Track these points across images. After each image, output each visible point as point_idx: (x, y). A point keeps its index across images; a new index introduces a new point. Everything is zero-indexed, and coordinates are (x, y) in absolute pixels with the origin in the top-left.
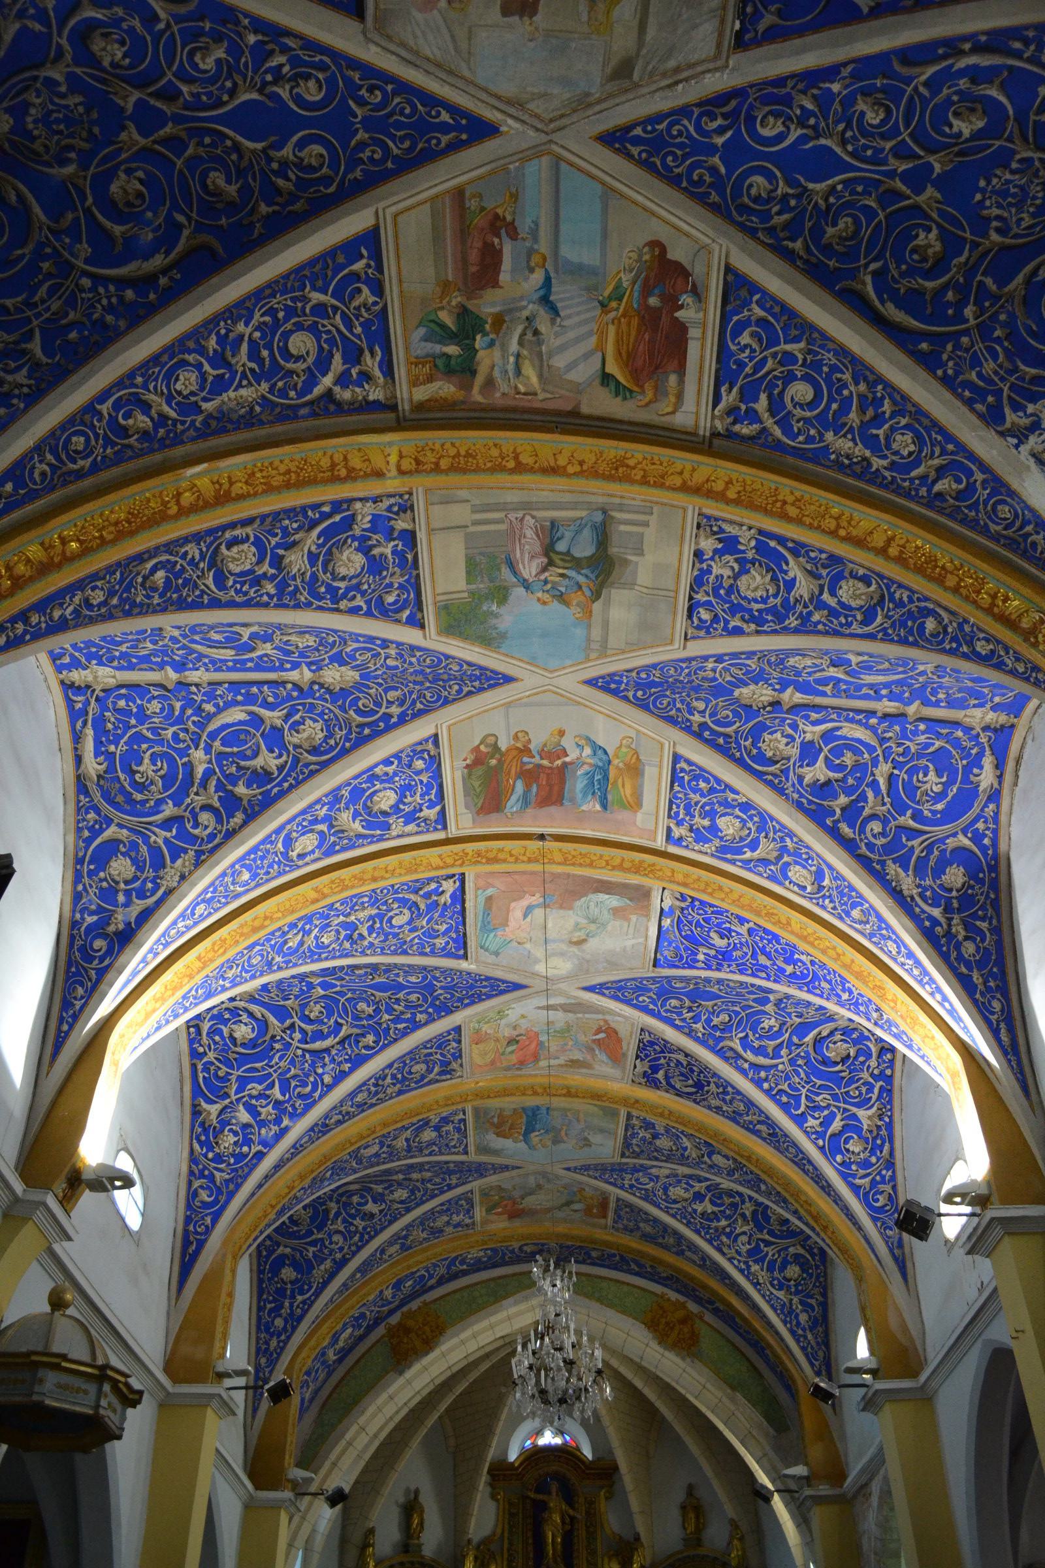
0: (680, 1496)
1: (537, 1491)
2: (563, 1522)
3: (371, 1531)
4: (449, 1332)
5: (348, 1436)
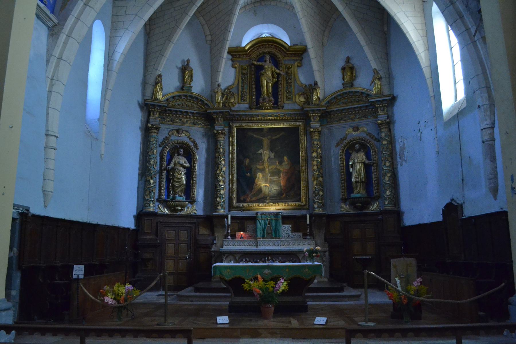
0: (341, 63)
1: (258, 61)
2: (273, 77)
3: (160, 76)
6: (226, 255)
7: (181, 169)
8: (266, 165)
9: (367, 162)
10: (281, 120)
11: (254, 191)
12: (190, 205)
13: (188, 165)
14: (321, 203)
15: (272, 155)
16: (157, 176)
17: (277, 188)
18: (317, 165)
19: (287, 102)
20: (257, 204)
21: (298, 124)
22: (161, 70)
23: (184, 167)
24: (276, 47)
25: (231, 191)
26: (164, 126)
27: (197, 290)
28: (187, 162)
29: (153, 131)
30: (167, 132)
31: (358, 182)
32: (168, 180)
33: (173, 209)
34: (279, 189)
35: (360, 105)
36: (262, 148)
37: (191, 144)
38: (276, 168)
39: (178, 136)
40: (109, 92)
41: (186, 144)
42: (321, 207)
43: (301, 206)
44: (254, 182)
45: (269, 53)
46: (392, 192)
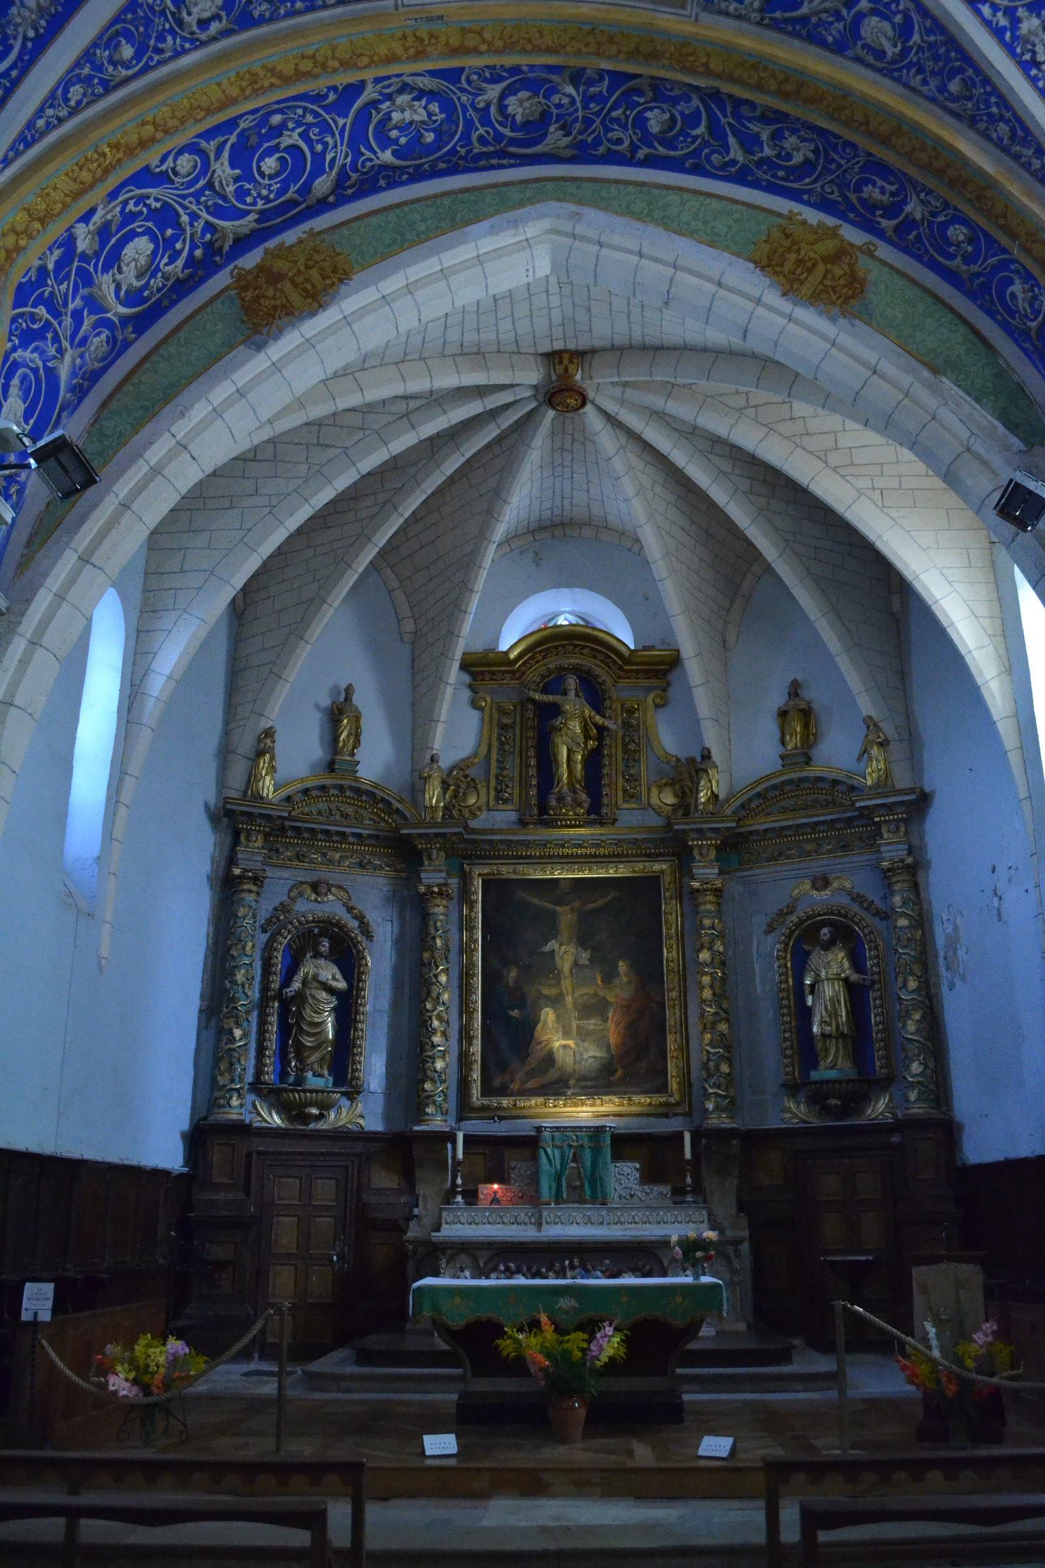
0: (777, 698)
1: (545, 691)
2: (587, 737)
3: (269, 733)
4: (357, 278)
5: (155, 454)
6: (449, 1252)
7: (323, 995)
8: (566, 984)
9: (855, 977)
10: (609, 856)
11: (532, 1062)
12: (345, 1102)
13: (341, 985)
14: (725, 1097)
15: (585, 957)
16: (254, 1018)
17: (598, 1054)
18: (712, 987)
19: (625, 806)
20: (540, 1100)
21: (657, 867)
22: (274, 713)
23: (331, 990)
24: (594, 654)
25: (464, 1060)
26: (279, 873)
27: (365, 1357)
28: (339, 976)
29: (245, 887)
30: (285, 890)
31: (830, 1036)
32: (285, 1030)
33: (294, 1112)
34: (604, 1055)
35: (829, 817)
36: (555, 937)
37: (353, 924)
38: (595, 995)
39: (316, 901)
40: (129, 782)
41: (338, 924)
42: (723, 1110)
43: (667, 1104)
44: (532, 1035)
45: (576, 670)
46: (926, 1065)
